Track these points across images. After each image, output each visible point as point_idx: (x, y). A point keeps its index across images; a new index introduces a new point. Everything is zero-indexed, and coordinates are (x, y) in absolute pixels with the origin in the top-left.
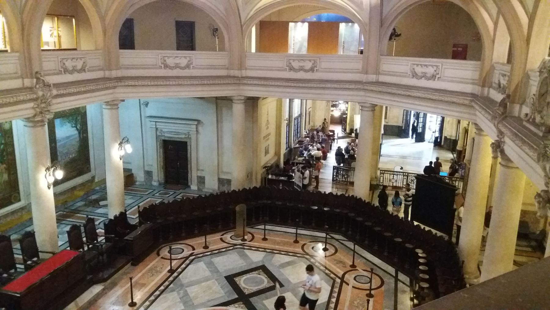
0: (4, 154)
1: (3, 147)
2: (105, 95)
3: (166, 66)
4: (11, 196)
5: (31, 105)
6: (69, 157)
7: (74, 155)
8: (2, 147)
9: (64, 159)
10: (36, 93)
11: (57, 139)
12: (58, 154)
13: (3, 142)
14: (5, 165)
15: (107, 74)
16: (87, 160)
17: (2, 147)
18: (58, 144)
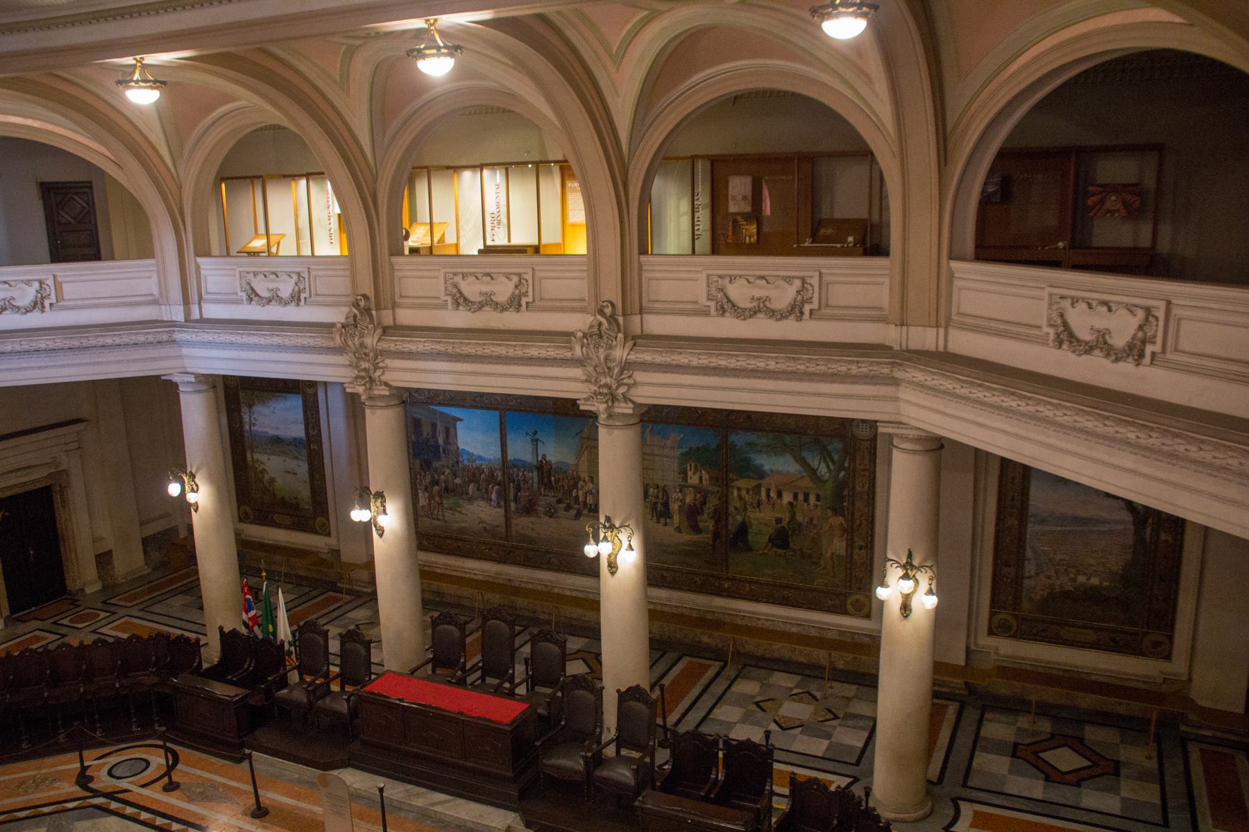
0: (845, 493)
1: (844, 476)
2: (875, 398)
3: (1066, 336)
4: (846, 595)
5: (578, 372)
6: (1074, 580)
7: (1095, 581)
8: (841, 475)
9: (1049, 577)
10: (571, 349)
11: (1032, 510)
12: (1029, 553)
13: (846, 465)
14: (841, 519)
15: (890, 335)
16: (1165, 618)
17: (841, 475)
18: (1032, 528)
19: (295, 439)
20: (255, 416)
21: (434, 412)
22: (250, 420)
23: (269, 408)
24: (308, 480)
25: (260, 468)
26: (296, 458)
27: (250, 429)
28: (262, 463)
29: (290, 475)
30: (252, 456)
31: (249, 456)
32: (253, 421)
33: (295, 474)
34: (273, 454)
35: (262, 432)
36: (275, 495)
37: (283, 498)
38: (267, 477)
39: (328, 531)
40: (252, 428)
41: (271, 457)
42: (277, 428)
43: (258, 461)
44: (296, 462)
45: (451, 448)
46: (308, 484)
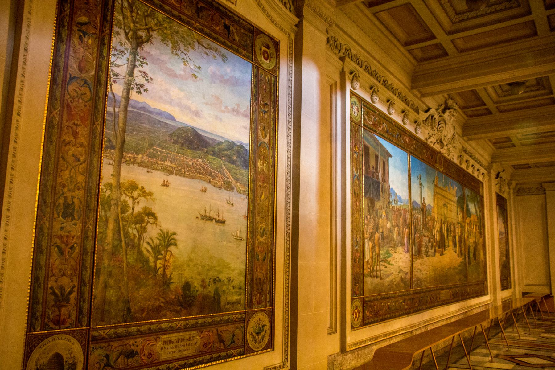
19: (231, 145)
20: (146, 68)
21: (377, 142)
22: (131, 73)
23: (185, 62)
24: (244, 236)
25: (138, 209)
26: (229, 187)
27: (127, 98)
28: (145, 193)
29: (210, 225)
30: (117, 174)
31: (107, 171)
32: (139, 79)
33: (223, 222)
34: (180, 174)
35: (160, 113)
36: (166, 282)
37: (187, 286)
38: (153, 232)
39: (266, 340)
40: (134, 95)
41: (173, 179)
42: (197, 114)
43: (133, 187)
44: (225, 195)
45: (386, 186)
46: (243, 246)
